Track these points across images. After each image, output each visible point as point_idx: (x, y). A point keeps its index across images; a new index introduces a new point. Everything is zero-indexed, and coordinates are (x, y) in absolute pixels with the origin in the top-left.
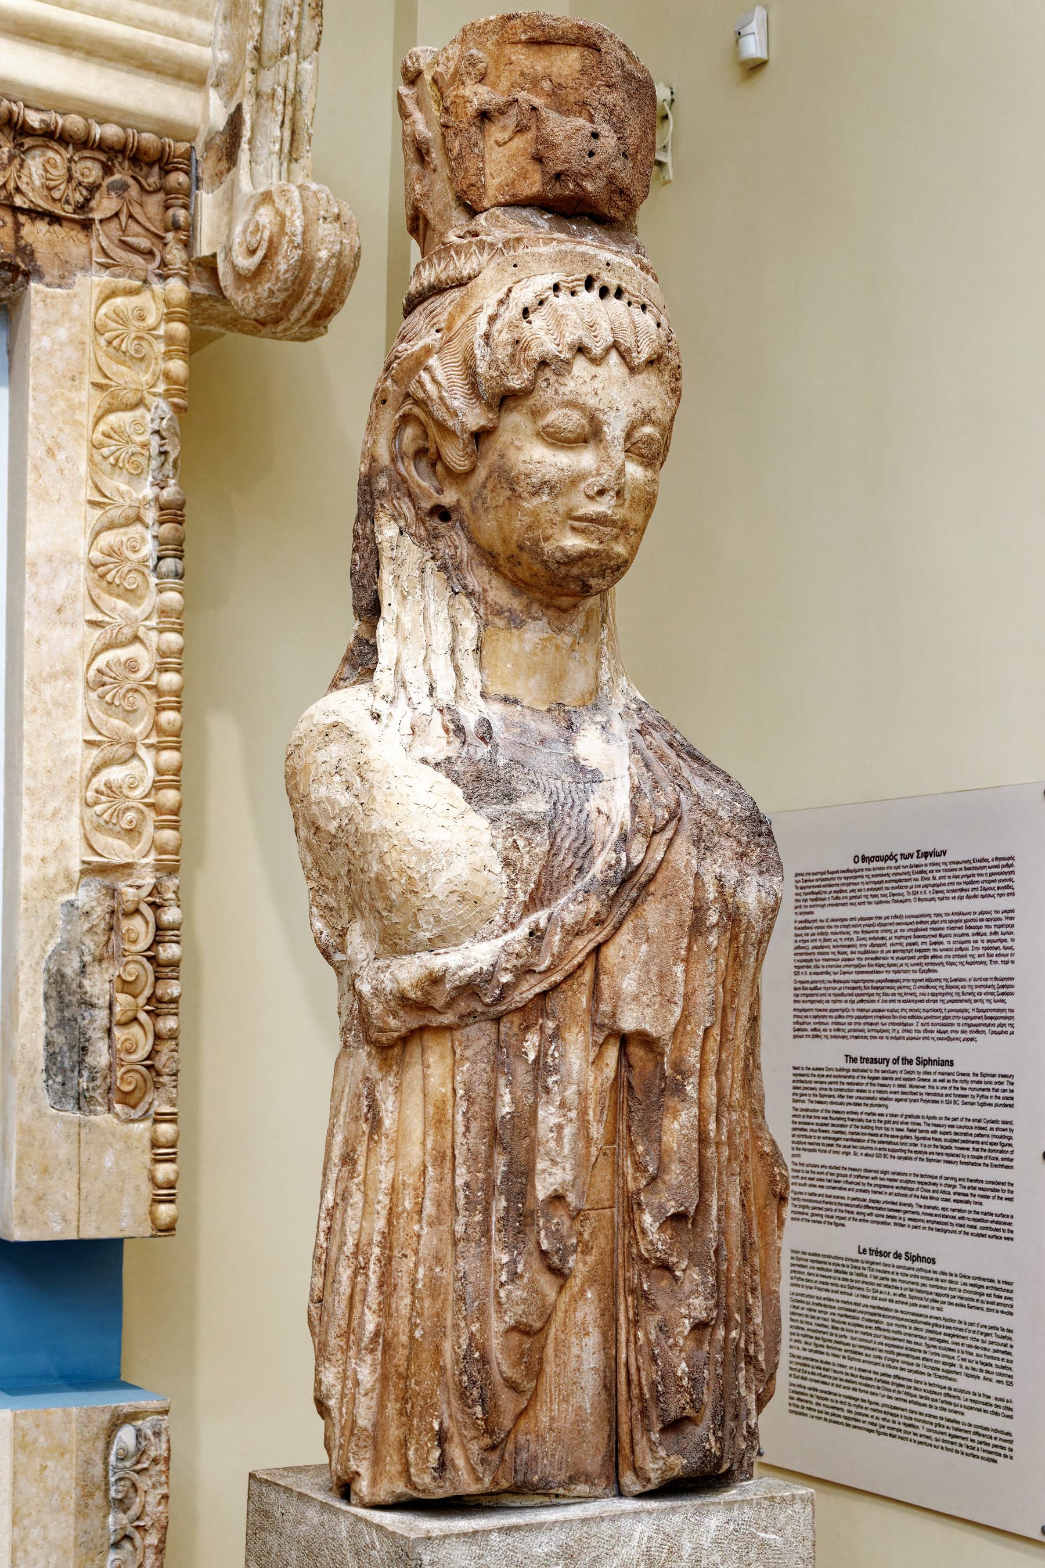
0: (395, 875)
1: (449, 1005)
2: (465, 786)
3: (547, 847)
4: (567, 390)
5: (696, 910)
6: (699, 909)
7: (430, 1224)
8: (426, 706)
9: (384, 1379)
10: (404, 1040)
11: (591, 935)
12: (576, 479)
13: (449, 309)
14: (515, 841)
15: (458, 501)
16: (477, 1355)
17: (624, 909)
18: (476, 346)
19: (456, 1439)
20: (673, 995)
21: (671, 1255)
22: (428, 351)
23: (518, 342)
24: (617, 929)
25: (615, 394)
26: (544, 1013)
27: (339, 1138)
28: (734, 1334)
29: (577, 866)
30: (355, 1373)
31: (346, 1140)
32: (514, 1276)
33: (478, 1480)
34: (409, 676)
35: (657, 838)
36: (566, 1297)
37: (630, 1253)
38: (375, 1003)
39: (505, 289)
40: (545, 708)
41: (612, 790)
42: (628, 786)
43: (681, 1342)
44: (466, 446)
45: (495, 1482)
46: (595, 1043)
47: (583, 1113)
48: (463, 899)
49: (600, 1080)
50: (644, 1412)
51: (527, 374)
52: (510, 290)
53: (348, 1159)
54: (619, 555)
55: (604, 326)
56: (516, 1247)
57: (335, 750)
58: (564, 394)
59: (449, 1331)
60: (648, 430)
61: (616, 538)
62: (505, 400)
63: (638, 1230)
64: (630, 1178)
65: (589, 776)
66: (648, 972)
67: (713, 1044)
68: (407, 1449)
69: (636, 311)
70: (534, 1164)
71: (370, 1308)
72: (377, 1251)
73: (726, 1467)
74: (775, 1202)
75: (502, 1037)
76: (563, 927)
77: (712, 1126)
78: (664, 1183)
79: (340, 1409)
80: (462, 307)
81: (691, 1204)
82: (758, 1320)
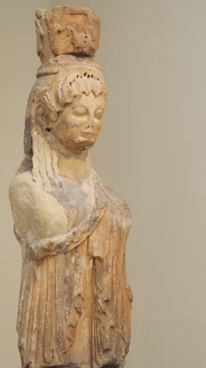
0: (42, 219)
1: (54, 250)
2: (57, 198)
3: (77, 213)
4: (80, 102)
5: (111, 227)
6: (112, 228)
7: (50, 302)
8: (46, 178)
9: (38, 339)
10: (42, 259)
11: (87, 233)
12: (82, 124)
13: (51, 80)
14: (69, 211)
15: (53, 127)
16: (61, 331)
17: (94, 227)
18: (59, 92)
19: (56, 352)
20: (106, 248)
21: (105, 310)
22: (46, 91)
23: (69, 91)
24: (93, 232)
25: (91, 103)
26: (76, 252)
27: (25, 283)
28: (120, 331)
29: (83, 217)
30: (31, 338)
31: (27, 284)
32: (70, 313)
33: (60, 361)
34: (41, 171)
35: (102, 210)
36: (80, 320)
37: (95, 310)
38: (36, 250)
39: (65, 77)
40: (74, 178)
41: (91, 198)
42: (94, 198)
43: (107, 331)
44: (55, 115)
45: (65, 362)
46: (88, 259)
47: (85, 275)
48: (58, 225)
49: (88, 268)
50: (99, 348)
51: (71, 99)
52: (66, 77)
53: (28, 288)
54: (92, 141)
55: (89, 86)
56: (70, 306)
57: (24, 189)
58: (80, 104)
59: (54, 326)
60: (99, 111)
61: (92, 137)
62: (66, 105)
63: (97, 304)
64: (95, 291)
65: (85, 195)
66: (100, 242)
67: (115, 260)
68: (44, 354)
69: (96, 80)
70: (74, 287)
71: (34, 323)
72: (36, 309)
73: (118, 363)
74: (129, 302)
75: (66, 257)
76: (81, 231)
77: (115, 279)
78: (103, 292)
79: (26, 348)
80: (54, 80)
81: (110, 298)
82: (125, 329)
